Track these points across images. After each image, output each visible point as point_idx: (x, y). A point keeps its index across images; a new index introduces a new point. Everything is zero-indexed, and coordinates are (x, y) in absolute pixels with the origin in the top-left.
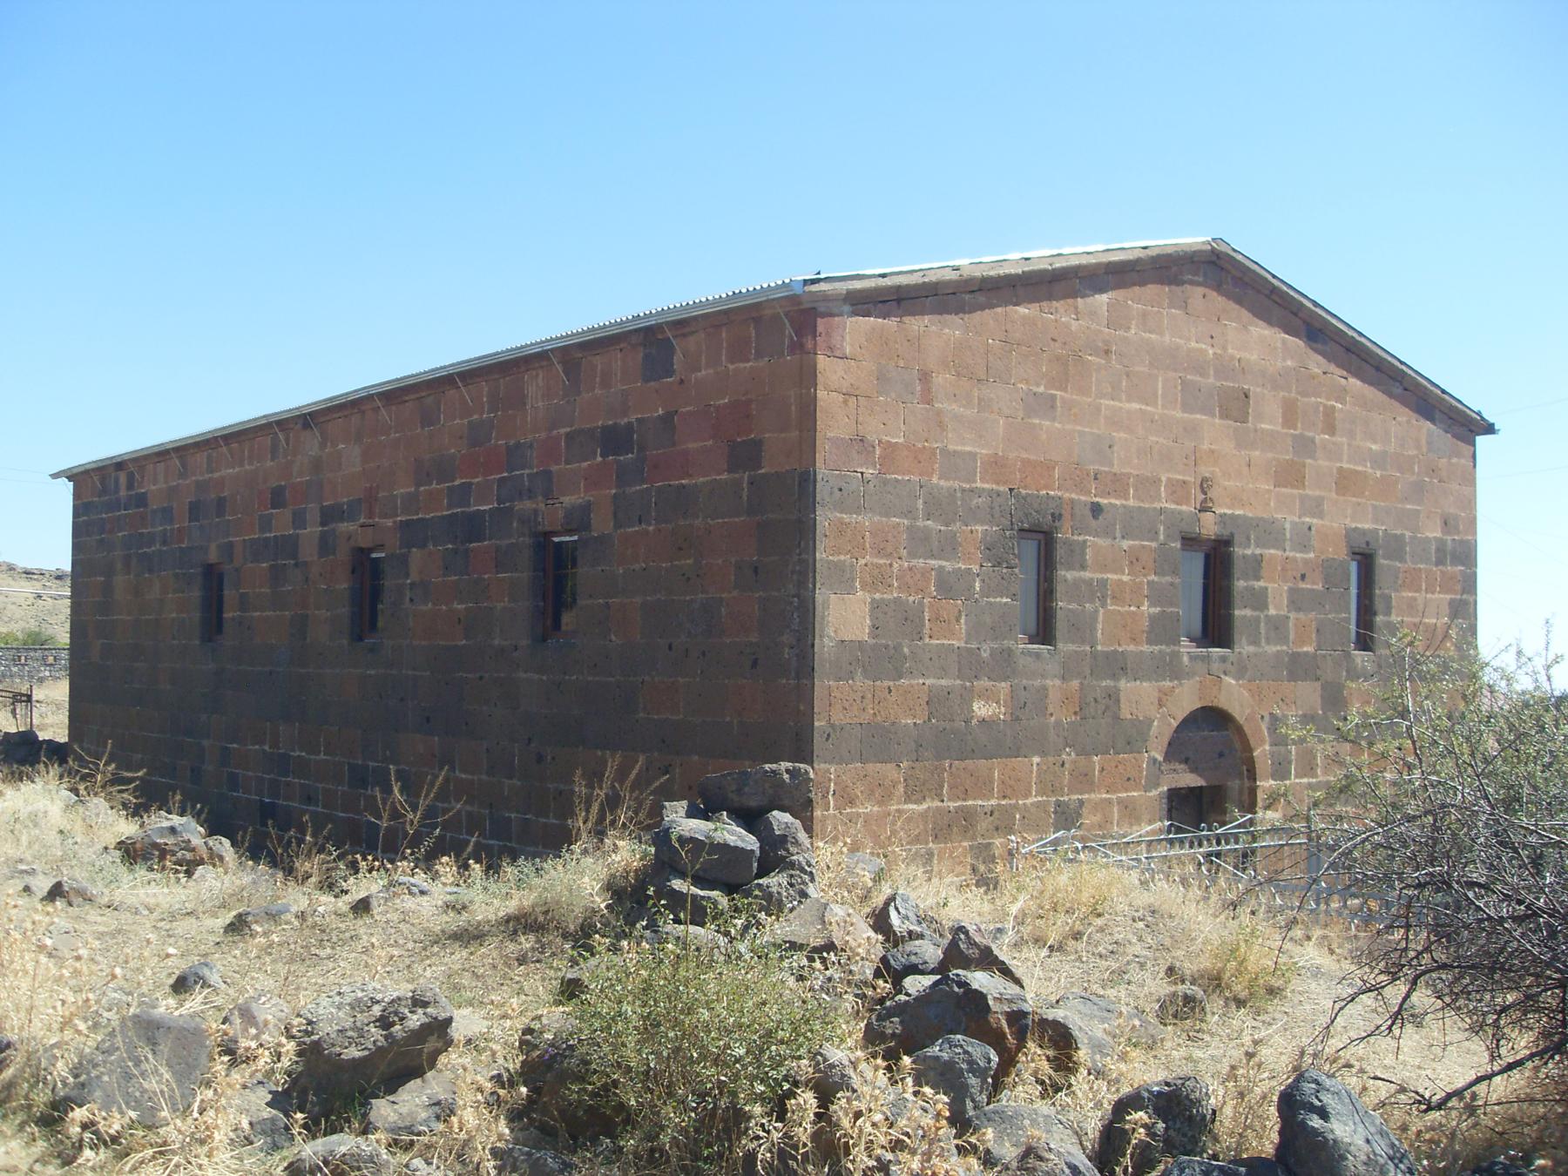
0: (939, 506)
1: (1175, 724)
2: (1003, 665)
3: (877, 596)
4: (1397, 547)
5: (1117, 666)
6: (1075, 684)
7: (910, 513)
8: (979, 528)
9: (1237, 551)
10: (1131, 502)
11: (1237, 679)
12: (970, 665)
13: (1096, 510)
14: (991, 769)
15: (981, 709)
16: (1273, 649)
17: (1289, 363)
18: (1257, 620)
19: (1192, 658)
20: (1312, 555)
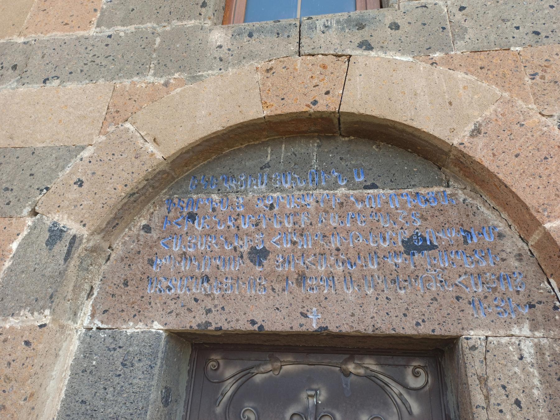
1: (157, 154)
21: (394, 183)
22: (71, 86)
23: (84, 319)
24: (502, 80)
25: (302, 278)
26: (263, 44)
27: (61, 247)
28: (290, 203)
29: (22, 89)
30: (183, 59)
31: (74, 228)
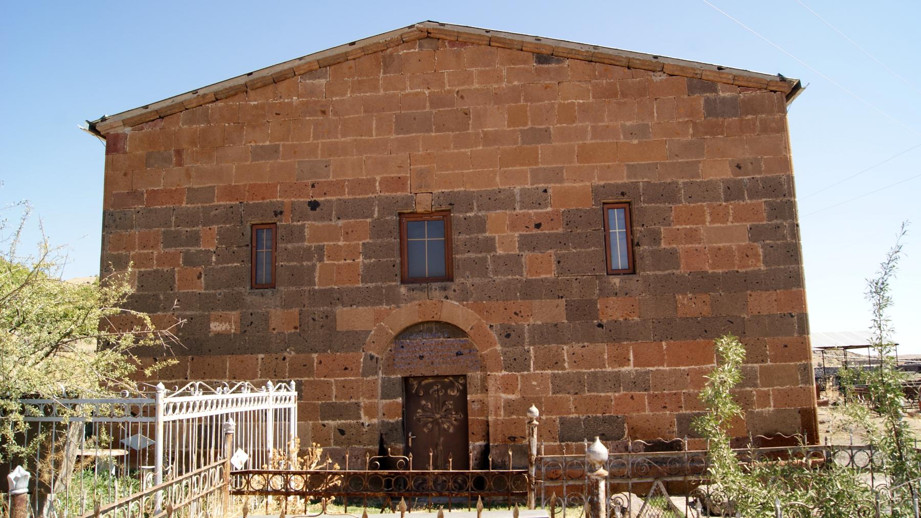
0: (190, 219)
2: (234, 302)
3: (142, 270)
4: (668, 194)
5: (332, 298)
6: (296, 310)
7: (167, 224)
8: (215, 227)
9: (456, 215)
10: (346, 197)
11: (461, 300)
12: (208, 303)
13: (314, 205)
14: (224, 363)
15: (216, 327)
16: (499, 278)
17: (516, 83)
18: (485, 258)
19: (409, 290)
20: (549, 209)
21: (455, 337)
22: (360, 308)
23: (381, 375)
24: (480, 312)
25: (432, 363)
26: (416, 294)
27: (374, 360)
28: (428, 342)
29: (345, 309)
30: (392, 299)
31: (376, 356)
